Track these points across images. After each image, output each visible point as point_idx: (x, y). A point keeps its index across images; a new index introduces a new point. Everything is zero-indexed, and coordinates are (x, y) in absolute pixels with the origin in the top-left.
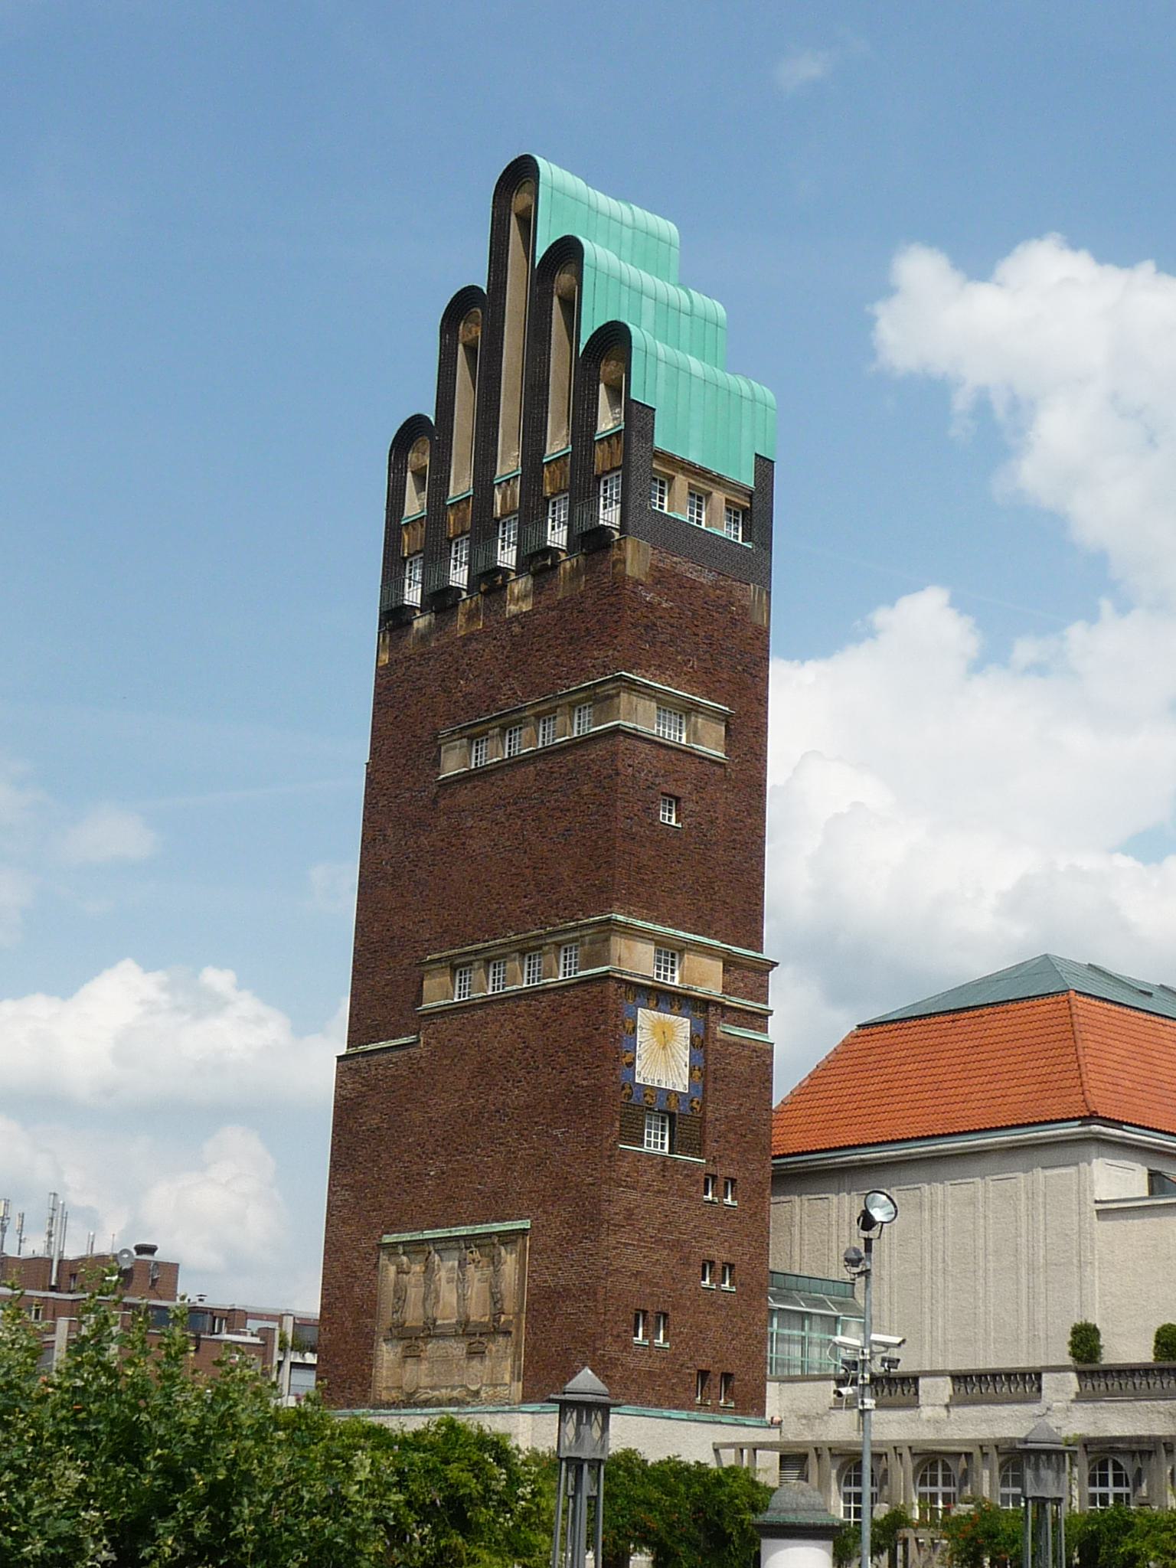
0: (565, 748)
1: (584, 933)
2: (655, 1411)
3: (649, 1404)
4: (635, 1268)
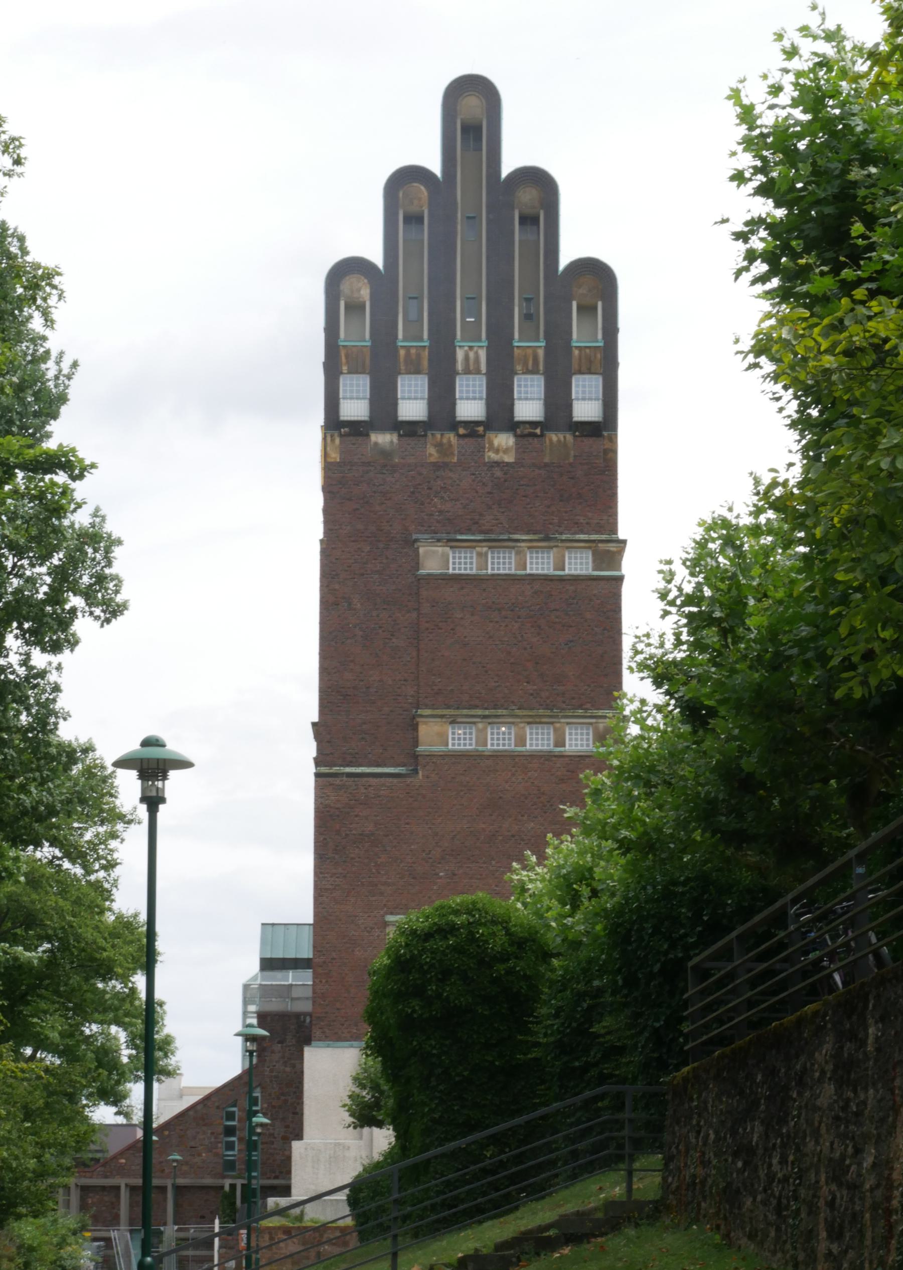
0: (564, 580)
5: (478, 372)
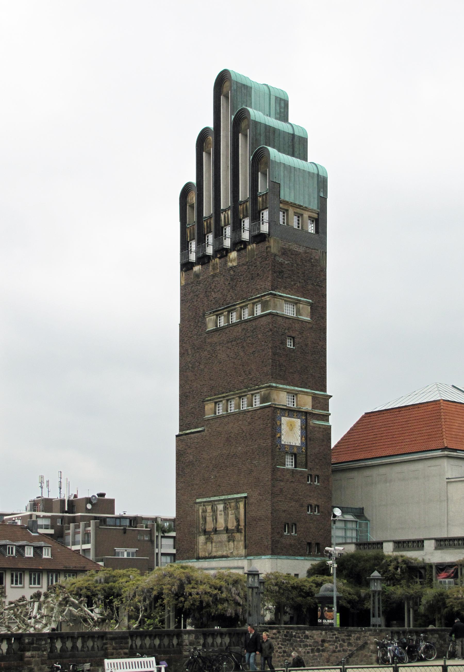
0: (251, 320)
1: (261, 390)
2: (293, 557)
3: (290, 555)
4: (284, 509)
5: (228, 224)
